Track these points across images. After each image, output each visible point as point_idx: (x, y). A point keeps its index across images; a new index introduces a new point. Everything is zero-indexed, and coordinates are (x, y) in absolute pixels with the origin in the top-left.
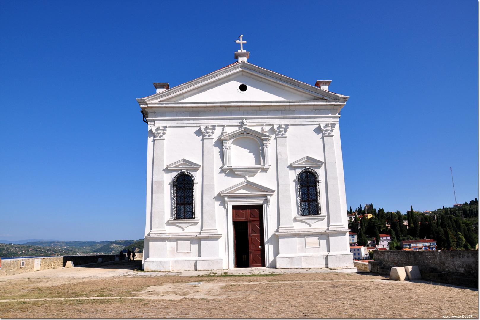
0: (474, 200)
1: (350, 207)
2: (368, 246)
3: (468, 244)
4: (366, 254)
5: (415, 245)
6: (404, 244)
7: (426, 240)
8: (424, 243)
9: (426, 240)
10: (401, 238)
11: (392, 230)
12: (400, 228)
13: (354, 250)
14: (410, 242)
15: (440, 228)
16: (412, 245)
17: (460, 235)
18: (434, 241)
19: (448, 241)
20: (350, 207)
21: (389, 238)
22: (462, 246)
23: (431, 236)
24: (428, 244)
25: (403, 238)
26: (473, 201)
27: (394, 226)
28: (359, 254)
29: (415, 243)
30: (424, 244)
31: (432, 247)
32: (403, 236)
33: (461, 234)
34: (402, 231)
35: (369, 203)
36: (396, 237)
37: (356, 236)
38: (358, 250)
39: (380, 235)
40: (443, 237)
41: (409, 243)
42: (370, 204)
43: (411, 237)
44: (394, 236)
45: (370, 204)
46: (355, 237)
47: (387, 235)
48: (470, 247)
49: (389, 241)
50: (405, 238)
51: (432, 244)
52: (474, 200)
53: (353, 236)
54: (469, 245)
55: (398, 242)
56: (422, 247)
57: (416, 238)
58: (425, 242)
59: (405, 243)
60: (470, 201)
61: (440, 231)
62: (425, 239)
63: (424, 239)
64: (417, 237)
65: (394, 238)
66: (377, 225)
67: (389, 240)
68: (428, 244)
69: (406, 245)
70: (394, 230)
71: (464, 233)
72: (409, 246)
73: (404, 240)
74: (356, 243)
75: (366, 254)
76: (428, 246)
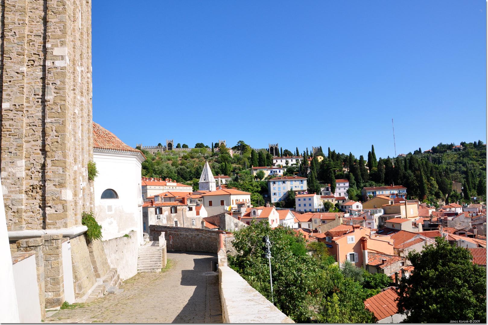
0: (418, 150)
1: (297, 148)
2: (321, 194)
3: (440, 191)
4: (320, 205)
5: (381, 193)
6: (367, 191)
7: (394, 186)
8: (392, 190)
9: (394, 186)
10: (362, 185)
11: (351, 174)
12: (361, 172)
13: (305, 200)
14: (374, 189)
15: (409, 171)
16: (377, 193)
17: (432, 180)
18: (404, 188)
19: (421, 187)
20: (297, 148)
21: (347, 184)
22: (433, 194)
23: (399, 181)
24: (396, 192)
25: (364, 184)
26: (417, 151)
27: (353, 170)
28: (310, 205)
29: (380, 191)
30: (392, 192)
31: (401, 195)
32: (364, 183)
33: (433, 179)
34: (362, 175)
35: (317, 146)
36: (356, 184)
37: (306, 181)
38: (310, 199)
39: (337, 180)
40: (414, 182)
41: (373, 191)
42: (318, 147)
43: (374, 183)
44: (353, 181)
45: (318, 147)
46: (305, 182)
47: (345, 180)
48: (442, 195)
49: (347, 189)
50: (367, 184)
51: (401, 192)
52: (418, 150)
53: (302, 181)
54: (442, 193)
55: (358, 189)
56: (389, 195)
57: (381, 184)
58: (392, 189)
59: (369, 190)
60: (415, 151)
61: (410, 176)
62: (392, 185)
63: (390, 185)
64: (381, 183)
65: (354, 184)
66: (332, 168)
67: (347, 187)
68: (396, 192)
69: (369, 193)
70: (353, 175)
71: (436, 178)
72: (373, 194)
73: (365, 186)
74: (305, 190)
75: (320, 205)
76: (397, 194)
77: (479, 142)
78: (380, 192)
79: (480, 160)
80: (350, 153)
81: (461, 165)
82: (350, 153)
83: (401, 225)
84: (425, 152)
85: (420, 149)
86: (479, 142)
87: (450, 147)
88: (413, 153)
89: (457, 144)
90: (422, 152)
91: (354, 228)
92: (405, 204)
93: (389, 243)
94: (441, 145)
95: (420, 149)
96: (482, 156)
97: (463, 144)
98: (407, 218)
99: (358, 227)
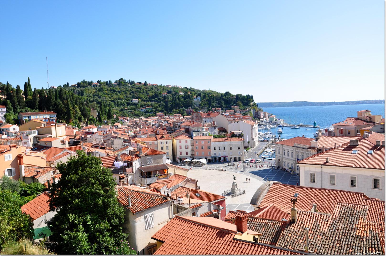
3: (82, 116)
5: (35, 117)
6: (23, 116)
7: (46, 112)
8: (44, 115)
9: (46, 112)
10: (19, 111)
11: (9, 101)
12: (18, 99)
14: (29, 114)
15: (59, 100)
16: (32, 117)
17: (76, 108)
18: (54, 114)
19: (68, 113)
21: (4, 110)
22: (77, 118)
23: (51, 108)
24: (48, 117)
25: (21, 110)
26: (66, 84)
27: (10, 97)
29: (35, 115)
30: (45, 116)
31: (53, 119)
32: (20, 109)
34: (19, 102)
36: (12, 109)
40: (63, 109)
41: (29, 116)
43: (29, 109)
44: (11, 107)
47: (2, 106)
48: (83, 119)
49: (4, 114)
50: (23, 110)
51: (52, 117)
52: (67, 84)
54: (83, 117)
55: (15, 114)
56: (42, 119)
57: (35, 110)
58: (45, 114)
59: (25, 115)
60: (64, 85)
61: (60, 104)
62: (45, 111)
63: (43, 111)
64: (36, 109)
65: (11, 109)
67: (4, 112)
68: (48, 117)
69: (25, 117)
70: (10, 101)
71: (80, 107)
72: (28, 118)
73: (21, 112)
76: (49, 118)
77: (110, 81)
78: (35, 117)
79: (110, 94)
80: (8, 82)
81: (97, 97)
82: (8, 82)
83: (52, 143)
84: (72, 86)
85: (68, 83)
86: (110, 81)
87: (90, 83)
88: (62, 86)
89: (95, 82)
90: (70, 86)
91: (11, 147)
92: (56, 126)
93: (42, 158)
94: (84, 82)
95: (68, 83)
96: (111, 92)
97: (99, 82)
98: (56, 137)
99: (15, 147)
